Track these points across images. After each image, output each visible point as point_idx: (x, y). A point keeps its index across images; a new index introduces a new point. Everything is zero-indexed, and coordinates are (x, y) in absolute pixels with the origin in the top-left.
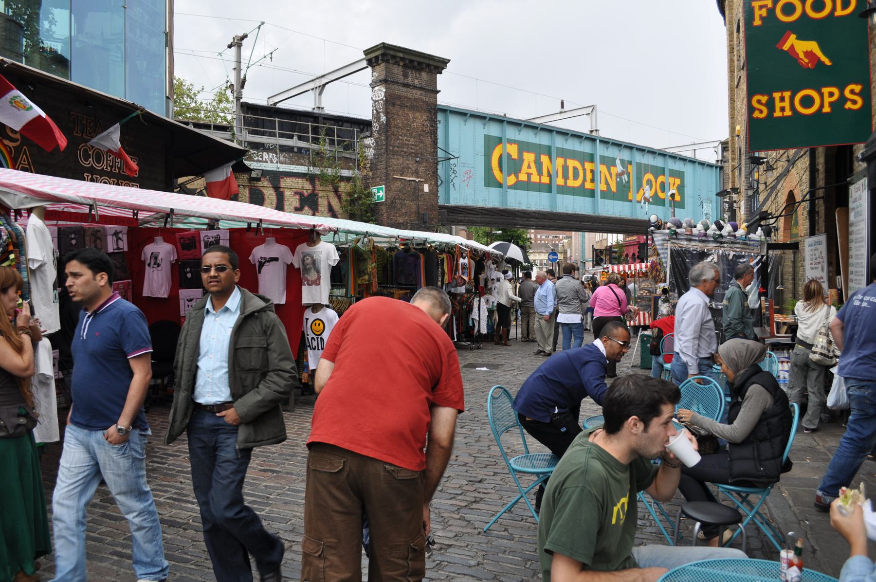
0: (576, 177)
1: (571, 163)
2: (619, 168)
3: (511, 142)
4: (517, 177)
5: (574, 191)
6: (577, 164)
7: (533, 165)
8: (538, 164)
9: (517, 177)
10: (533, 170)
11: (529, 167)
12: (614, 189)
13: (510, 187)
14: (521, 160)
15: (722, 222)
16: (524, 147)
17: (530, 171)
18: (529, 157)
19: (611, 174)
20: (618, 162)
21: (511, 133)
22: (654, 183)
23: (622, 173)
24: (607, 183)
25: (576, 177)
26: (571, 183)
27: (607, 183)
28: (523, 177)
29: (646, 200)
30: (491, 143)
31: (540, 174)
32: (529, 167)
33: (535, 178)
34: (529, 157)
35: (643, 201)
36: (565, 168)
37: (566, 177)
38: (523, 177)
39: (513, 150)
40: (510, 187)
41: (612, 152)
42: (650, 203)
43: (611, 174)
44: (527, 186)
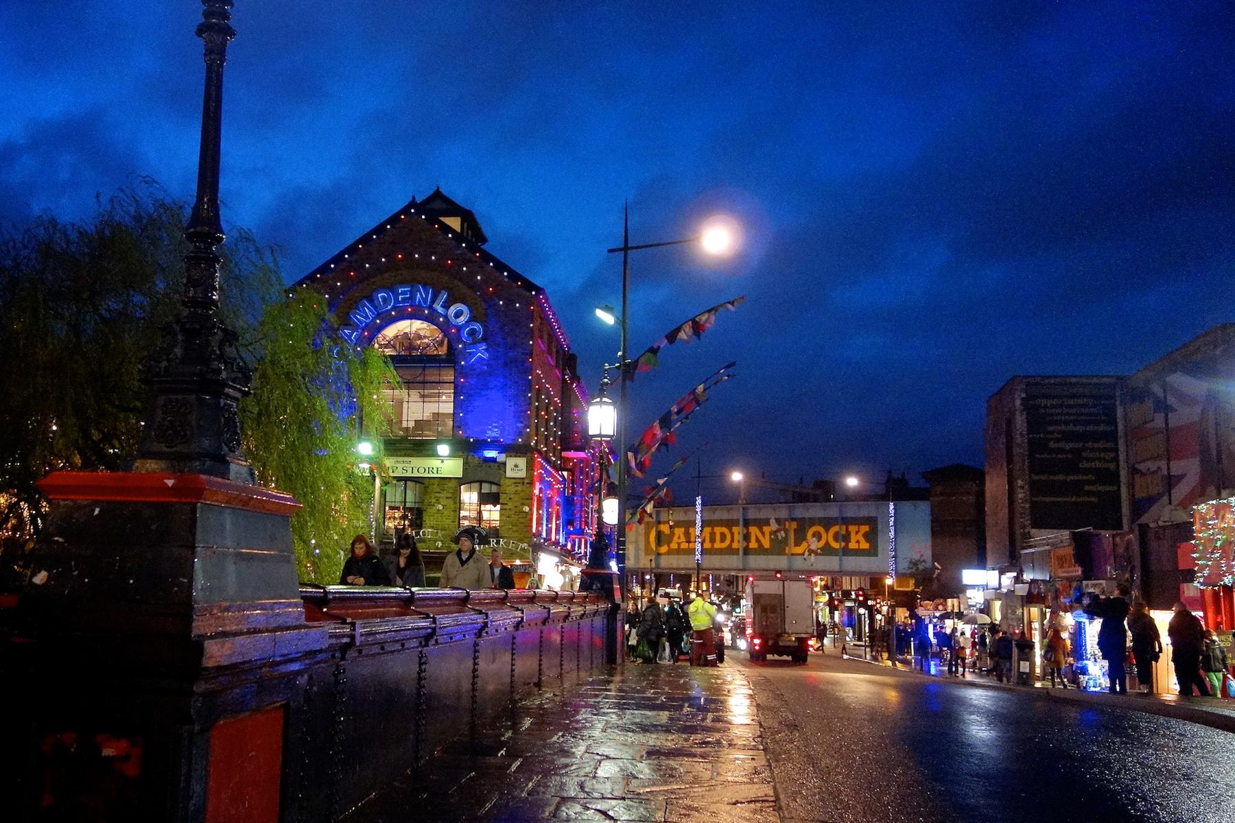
0: (723, 540)
1: (718, 530)
2: (774, 526)
5: (721, 552)
6: (725, 530)
10: (683, 539)
12: (766, 544)
14: (673, 534)
19: (763, 534)
20: (772, 521)
22: (824, 535)
23: (778, 531)
24: (758, 540)
25: (723, 540)
26: (718, 545)
27: (758, 540)
28: (674, 546)
29: (811, 552)
36: (712, 535)
37: (713, 541)
38: (674, 546)
39: (665, 528)
42: (816, 554)
43: (763, 534)
44: (679, 551)
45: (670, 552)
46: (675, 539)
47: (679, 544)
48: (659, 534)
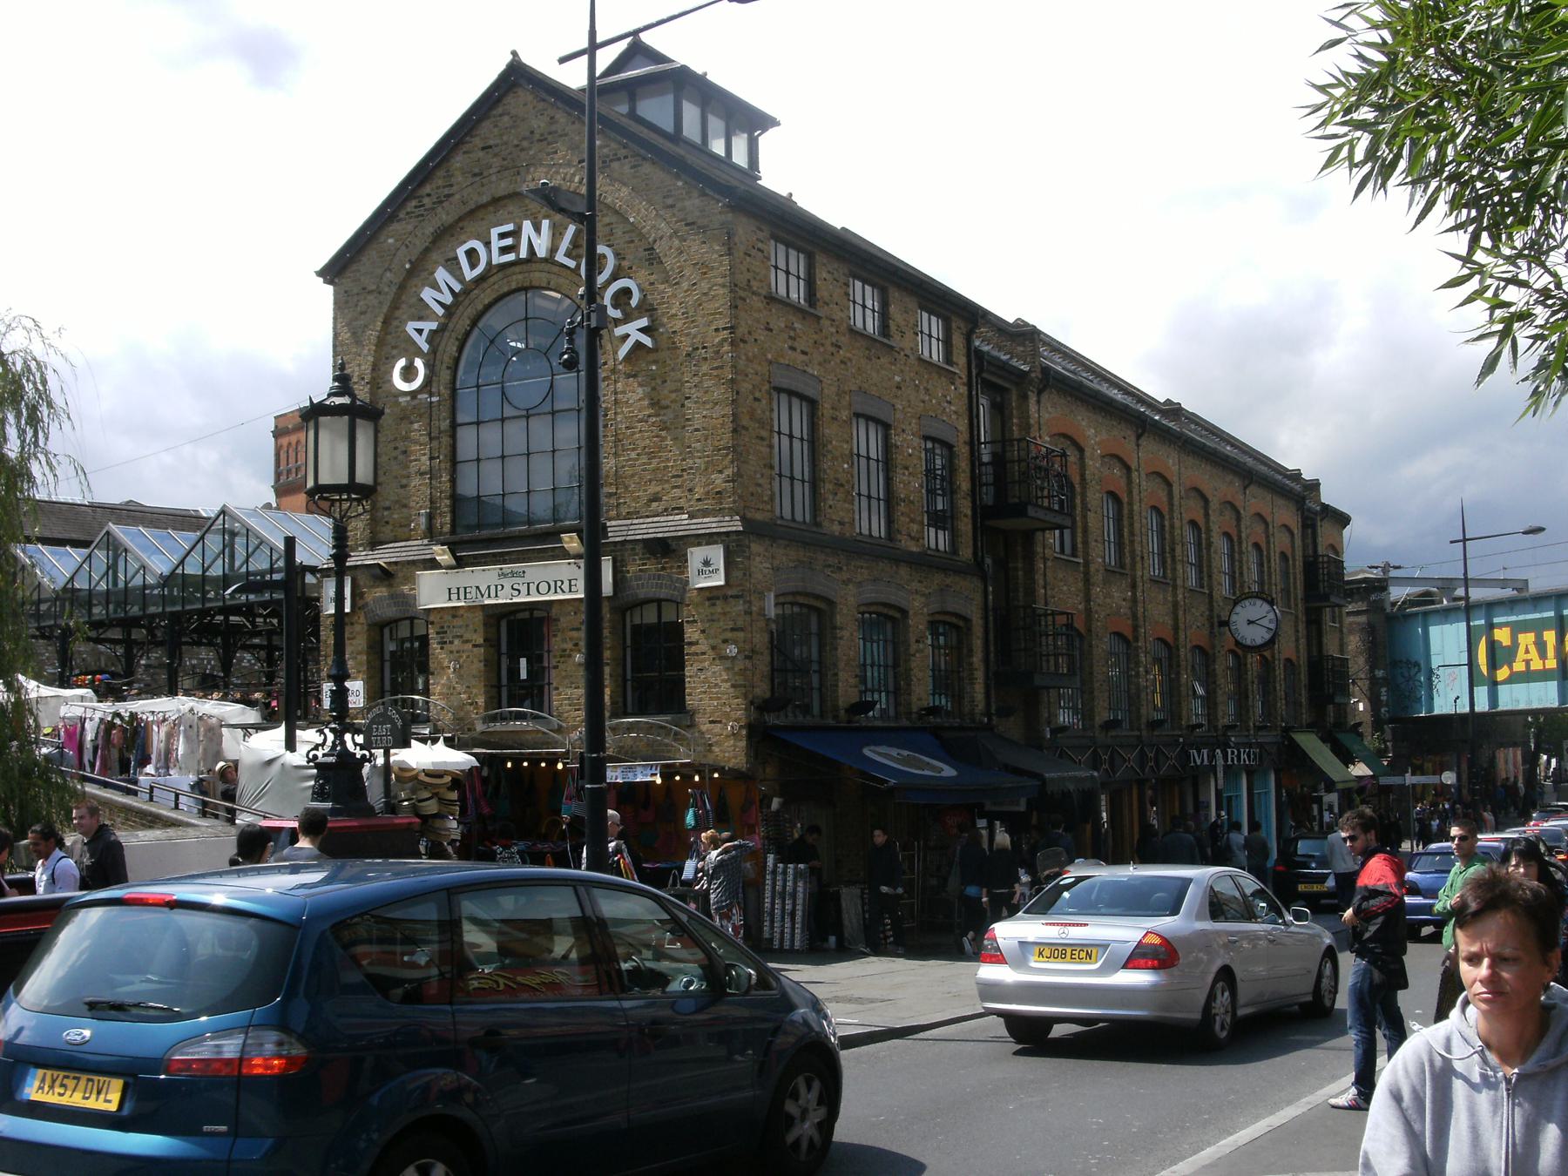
4: (1511, 667)
7: (1532, 649)
8: (1541, 646)
9: (1511, 667)
11: (1527, 652)
13: (1504, 682)
15: (1311, 744)
17: (1528, 657)
28: (1519, 666)
32: (1527, 652)
33: (1537, 665)
34: (1527, 639)
38: (1519, 666)
39: (1502, 636)
40: (1504, 682)
44: (1528, 676)
45: (1514, 678)
46: (1521, 654)
47: (1528, 662)
48: (1492, 646)
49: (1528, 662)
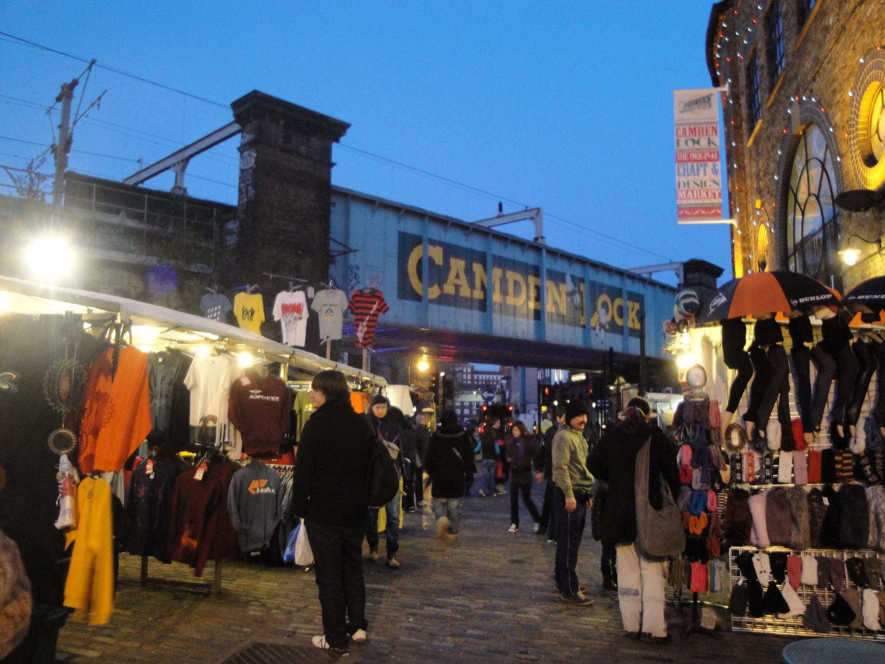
3: (433, 243)
4: (441, 288)
7: (462, 275)
8: (469, 272)
9: (441, 288)
10: (463, 281)
11: (457, 277)
14: (447, 267)
16: (450, 251)
17: (458, 282)
18: (458, 265)
20: (568, 278)
21: (435, 232)
24: (555, 303)
28: (449, 289)
29: (602, 326)
30: (407, 243)
31: (472, 286)
32: (457, 277)
34: (458, 265)
35: (598, 328)
38: (449, 289)
39: (437, 254)
40: (432, 301)
41: (560, 266)
42: (606, 330)
44: (454, 301)
45: (443, 300)
47: (457, 287)
49: (457, 287)
